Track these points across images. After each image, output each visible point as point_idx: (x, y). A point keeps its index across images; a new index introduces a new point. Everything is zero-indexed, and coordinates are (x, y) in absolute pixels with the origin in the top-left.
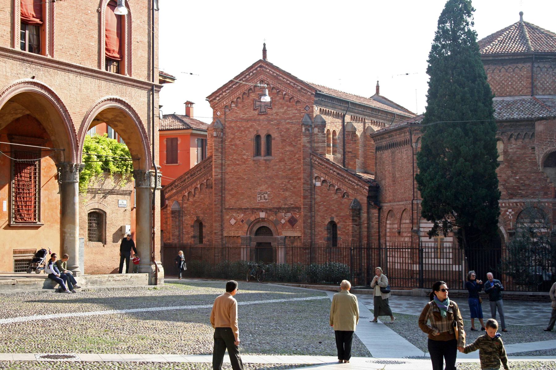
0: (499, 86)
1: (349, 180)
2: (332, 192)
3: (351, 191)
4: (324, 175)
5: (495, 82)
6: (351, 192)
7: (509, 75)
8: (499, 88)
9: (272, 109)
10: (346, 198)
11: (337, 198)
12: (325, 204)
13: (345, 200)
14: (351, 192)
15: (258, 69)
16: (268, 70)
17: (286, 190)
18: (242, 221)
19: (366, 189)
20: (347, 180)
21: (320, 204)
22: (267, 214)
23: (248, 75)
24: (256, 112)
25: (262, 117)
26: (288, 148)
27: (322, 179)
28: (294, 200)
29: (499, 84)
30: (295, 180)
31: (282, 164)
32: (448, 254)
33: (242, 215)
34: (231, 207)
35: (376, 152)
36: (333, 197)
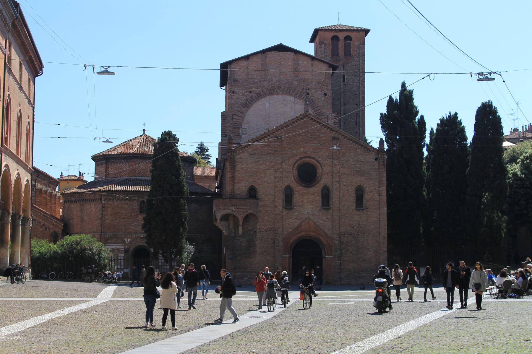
0: (143, 171)
1: (51, 219)
2: (39, 226)
3: (51, 226)
5: (140, 169)
7: (148, 166)
8: (142, 172)
10: (48, 230)
11: (41, 230)
12: (34, 233)
13: (47, 231)
14: (51, 226)
20: (49, 219)
29: (143, 170)
32: (121, 263)
35: (64, 203)
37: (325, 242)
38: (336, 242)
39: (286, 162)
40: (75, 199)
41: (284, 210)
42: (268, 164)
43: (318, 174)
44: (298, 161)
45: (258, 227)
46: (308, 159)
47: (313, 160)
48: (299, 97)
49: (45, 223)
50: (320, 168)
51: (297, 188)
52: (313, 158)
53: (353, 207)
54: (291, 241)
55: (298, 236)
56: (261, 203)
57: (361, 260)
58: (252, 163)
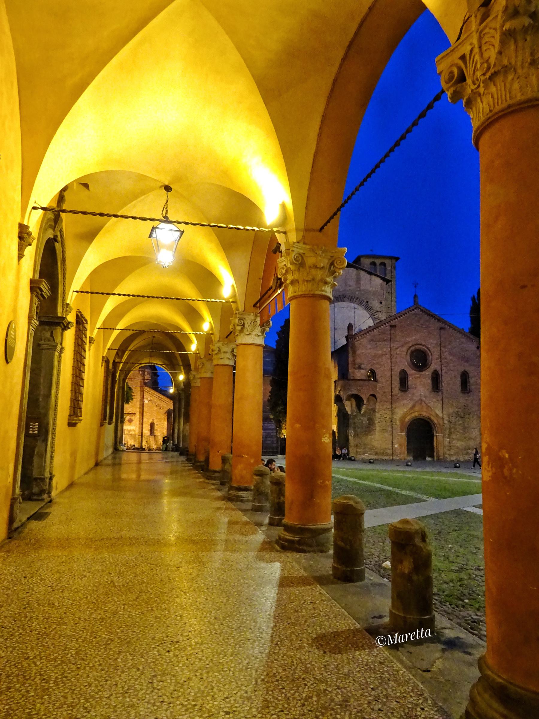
37: (436, 422)
38: (446, 422)
39: (400, 348)
41: (400, 392)
42: (385, 349)
43: (428, 361)
44: (410, 347)
45: (377, 407)
46: (419, 346)
47: (424, 347)
48: (360, 304)
50: (430, 354)
51: (411, 372)
52: (424, 345)
53: (460, 390)
54: (407, 420)
55: (413, 415)
56: (379, 385)
57: (467, 439)
58: (370, 348)
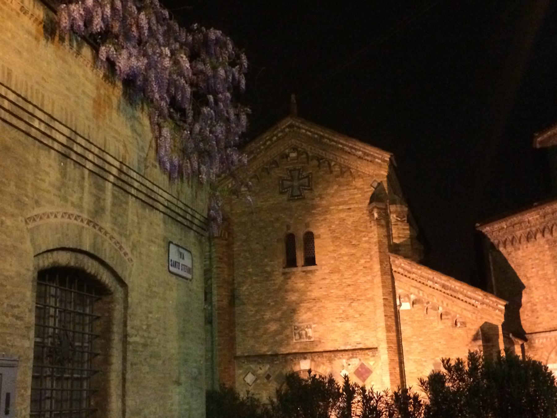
2: (432, 318)
4: (416, 291)
6: (469, 316)
9: (311, 189)
11: (443, 329)
14: (469, 316)
15: (287, 130)
16: (304, 131)
17: (347, 318)
18: (268, 377)
19: (500, 310)
21: (412, 340)
22: (313, 363)
23: (268, 140)
24: (285, 197)
25: (294, 205)
26: (345, 250)
27: (413, 297)
28: (362, 336)
30: (361, 302)
31: (335, 277)
33: (268, 366)
34: (246, 354)
36: (435, 327)
40: (528, 230)
49: (450, 307)
